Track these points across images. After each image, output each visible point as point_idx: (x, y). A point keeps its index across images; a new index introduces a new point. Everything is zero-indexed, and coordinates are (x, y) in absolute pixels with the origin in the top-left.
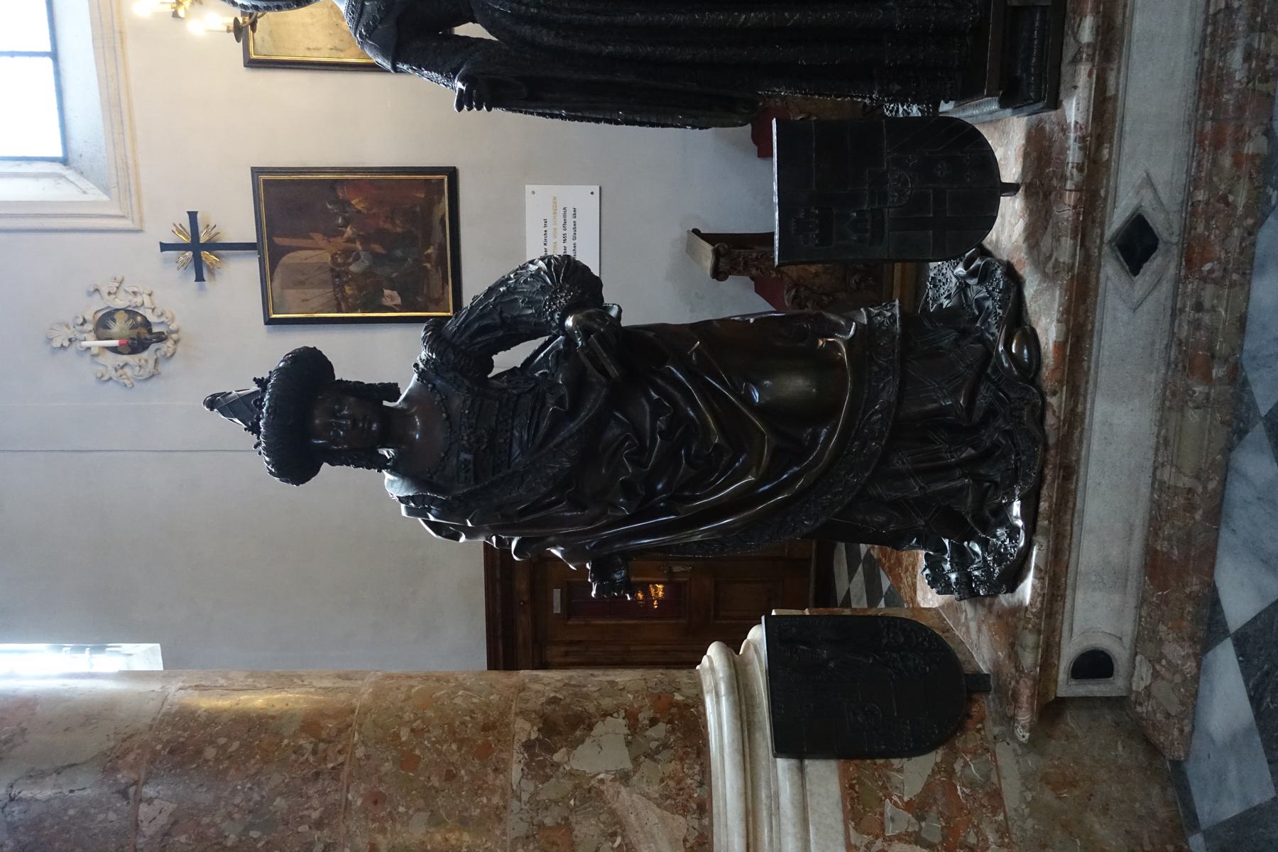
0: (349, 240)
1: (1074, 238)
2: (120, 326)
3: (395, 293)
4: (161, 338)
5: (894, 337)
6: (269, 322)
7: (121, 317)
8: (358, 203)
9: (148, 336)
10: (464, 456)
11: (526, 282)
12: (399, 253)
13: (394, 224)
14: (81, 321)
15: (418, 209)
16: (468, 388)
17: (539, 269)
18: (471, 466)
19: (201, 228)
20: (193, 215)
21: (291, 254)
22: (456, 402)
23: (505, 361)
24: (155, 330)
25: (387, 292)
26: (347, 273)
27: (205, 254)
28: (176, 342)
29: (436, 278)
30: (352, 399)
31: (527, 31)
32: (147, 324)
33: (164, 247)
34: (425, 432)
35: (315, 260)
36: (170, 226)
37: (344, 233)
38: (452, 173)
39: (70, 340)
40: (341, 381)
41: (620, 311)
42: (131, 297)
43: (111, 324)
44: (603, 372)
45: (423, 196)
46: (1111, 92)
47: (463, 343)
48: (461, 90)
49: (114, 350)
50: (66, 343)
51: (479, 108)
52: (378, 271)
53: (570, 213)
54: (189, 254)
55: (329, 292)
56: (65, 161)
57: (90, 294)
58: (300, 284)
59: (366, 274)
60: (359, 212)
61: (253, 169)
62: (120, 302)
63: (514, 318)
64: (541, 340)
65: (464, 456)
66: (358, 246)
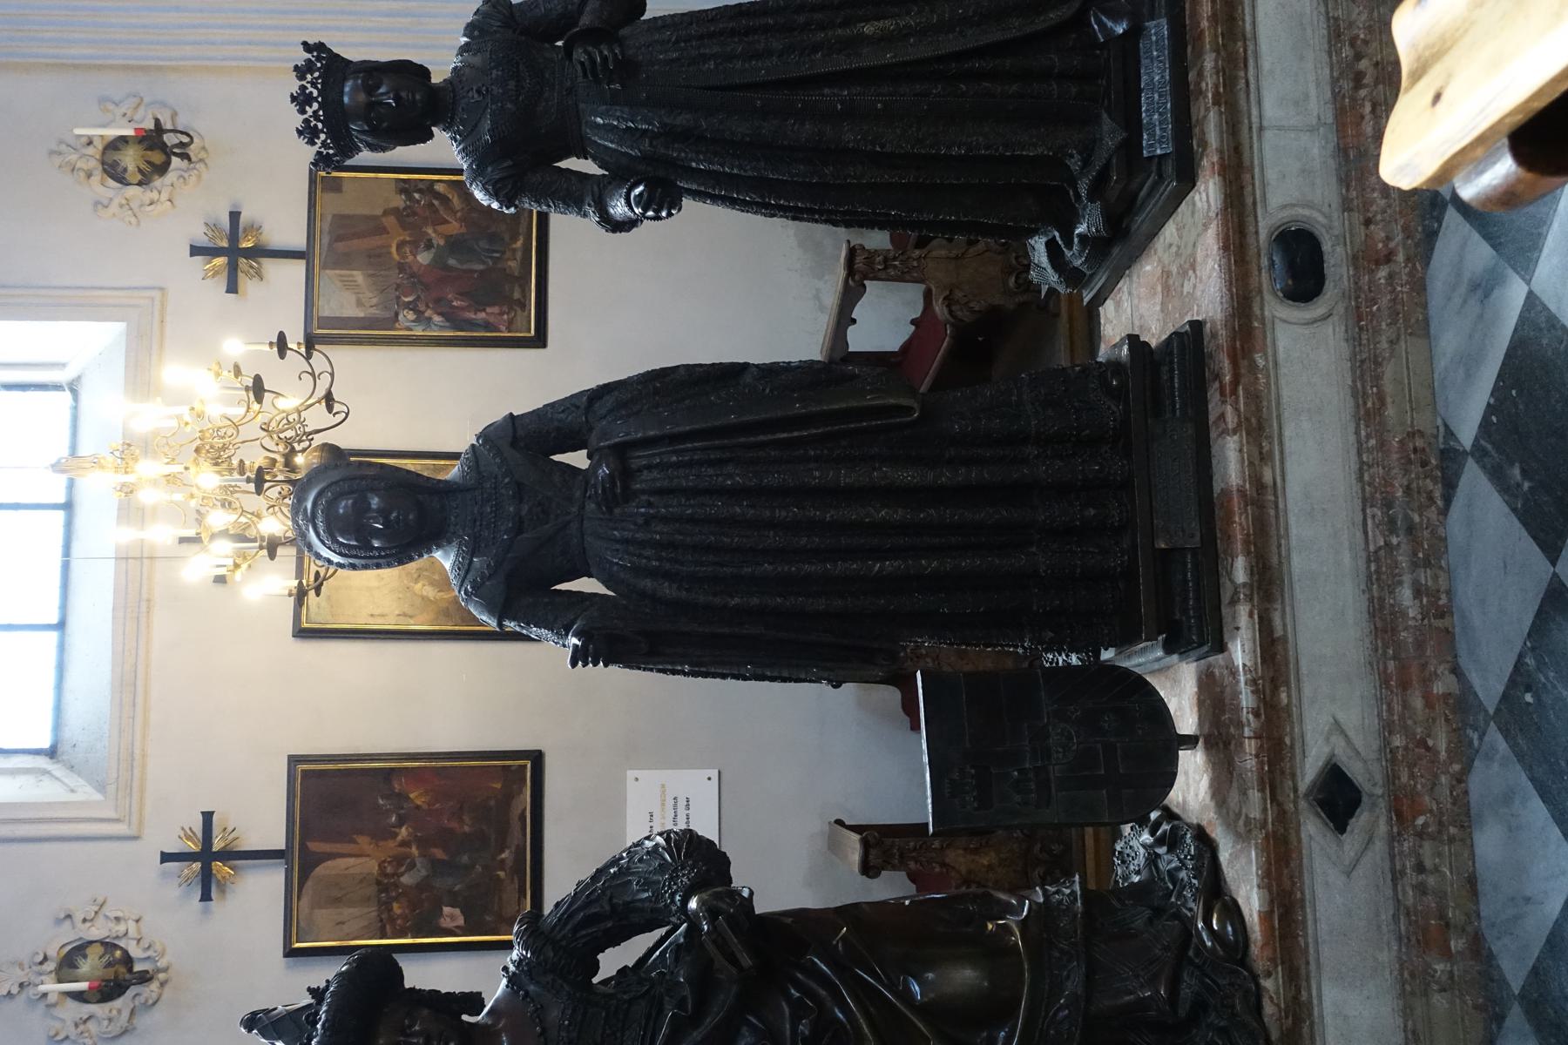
0: (404, 844)
1: (1262, 790)
2: (90, 965)
3: (457, 911)
4: (145, 978)
5: (1075, 916)
6: (290, 953)
7: (94, 953)
8: (417, 797)
9: (128, 976)
11: (641, 860)
12: (465, 859)
14: (40, 958)
15: (492, 803)
17: (657, 845)
19: (216, 830)
20: (208, 817)
22: (554, 1014)
23: (611, 962)
24: (137, 968)
25: (446, 910)
26: (396, 886)
28: (163, 984)
29: (511, 889)
30: (425, 1012)
31: (647, 584)
32: (128, 960)
33: (166, 857)
37: (396, 835)
38: (537, 758)
39: (21, 985)
40: (412, 990)
41: (751, 893)
42: (111, 925)
43: (81, 962)
44: (734, 961)
45: (498, 786)
46: (1279, 632)
48: (576, 646)
49: (79, 996)
50: (15, 990)
51: (595, 665)
52: (437, 883)
53: (682, 804)
54: (197, 866)
55: (371, 911)
56: (52, 753)
57: (59, 922)
58: (336, 901)
59: (422, 886)
60: (418, 807)
61: (290, 757)
62: (96, 932)
63: (627, 904)
64: (663, 931)
66: (414, 850)
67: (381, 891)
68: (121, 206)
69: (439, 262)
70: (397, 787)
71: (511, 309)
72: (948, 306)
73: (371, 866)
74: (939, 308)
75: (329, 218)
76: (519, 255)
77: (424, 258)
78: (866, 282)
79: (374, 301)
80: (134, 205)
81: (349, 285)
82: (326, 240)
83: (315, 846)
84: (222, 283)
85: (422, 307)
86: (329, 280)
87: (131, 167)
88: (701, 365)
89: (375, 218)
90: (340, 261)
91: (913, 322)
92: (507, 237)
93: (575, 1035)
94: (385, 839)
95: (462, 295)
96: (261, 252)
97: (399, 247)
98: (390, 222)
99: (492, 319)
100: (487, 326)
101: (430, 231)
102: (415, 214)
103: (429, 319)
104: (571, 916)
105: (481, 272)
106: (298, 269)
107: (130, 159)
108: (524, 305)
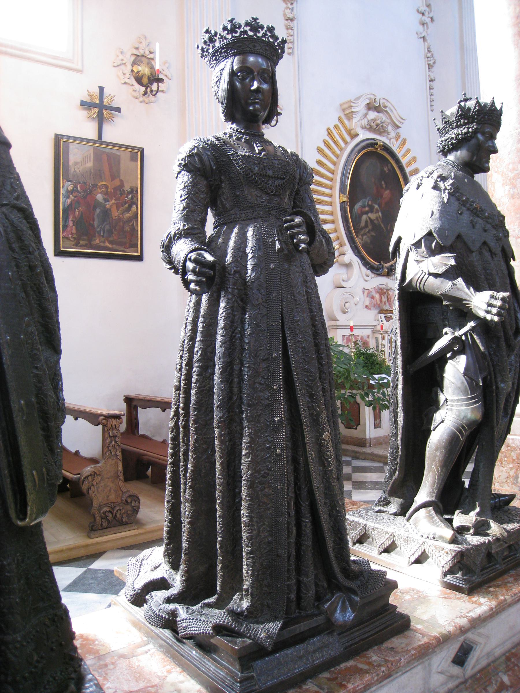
68: (122, 60)
69: (97, 204)
71: (75, 239)
72: (91, 475)
74: (89, 469)
75: (118, 154)
76: (102, 244)
77: (100, 197)
78: (101, 426)
79: (78, 171)
80: (123, 67)
81: (85, 160)
82: (108, 151)
84: (87, 99)
85: (75, 194)
86: (88, 150)
87: (140, 68)
88: (57, 311)
89: (119, 176)
90: (98, 156)
91: (77, 452)
92: (111, 239)
95: (82, 214)
96: (101, 120)
97: (106, 187)
98: (117, 183)
99: (69, 229)
100: (65, 226)
101: (113, 201)
102: (121, 194)
103: (68, 197)
105: (93, 226)
106: (94, 136)
107: (143, 69)
108: (77, 245)
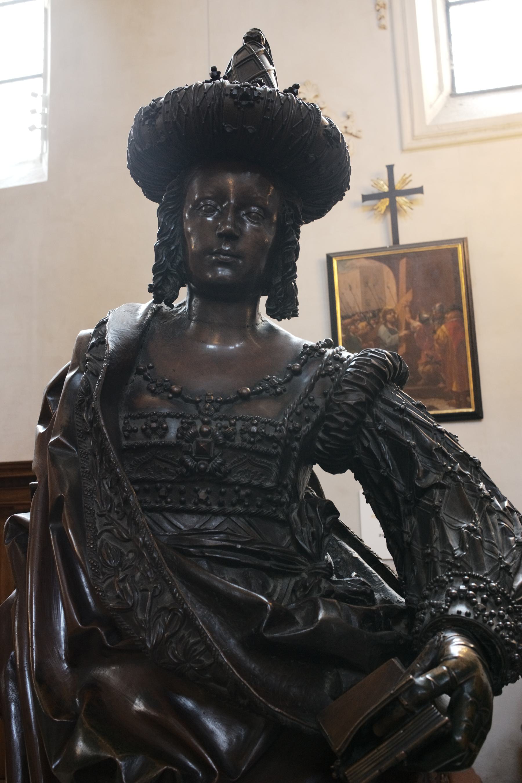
0: (408, 326)
8: (443, 331)
10: (173, 427)
13: (426, 363)
15: (441, 385)
16: (296, 430)
18: (155, 440)
20: (420, 190)
21: (391, 275)
22: (266, 409)
23: (344, 492)
26: (378, 323)
27: (386, 202)
30: (269, 238)
33: (390, 169)
34: (221, 362)
35: (387, 294)
36: (407, 173)
37: (414, 318)
38: (477, 416)
45: (454, 389)
47: (377, 420)
54: (386, 189)
55: (359, 307)
58: (365, 283)
60: (435, 332)
63: (435, 510)
64: (392, 566)
65: (173, 427)
66: (403, 333)
67: (373, 312)
70: (448, 316)
73: (391, 304)
83: (403, 264)
93: (238, 441)
94: (411, 312)
104: (407, 426)
